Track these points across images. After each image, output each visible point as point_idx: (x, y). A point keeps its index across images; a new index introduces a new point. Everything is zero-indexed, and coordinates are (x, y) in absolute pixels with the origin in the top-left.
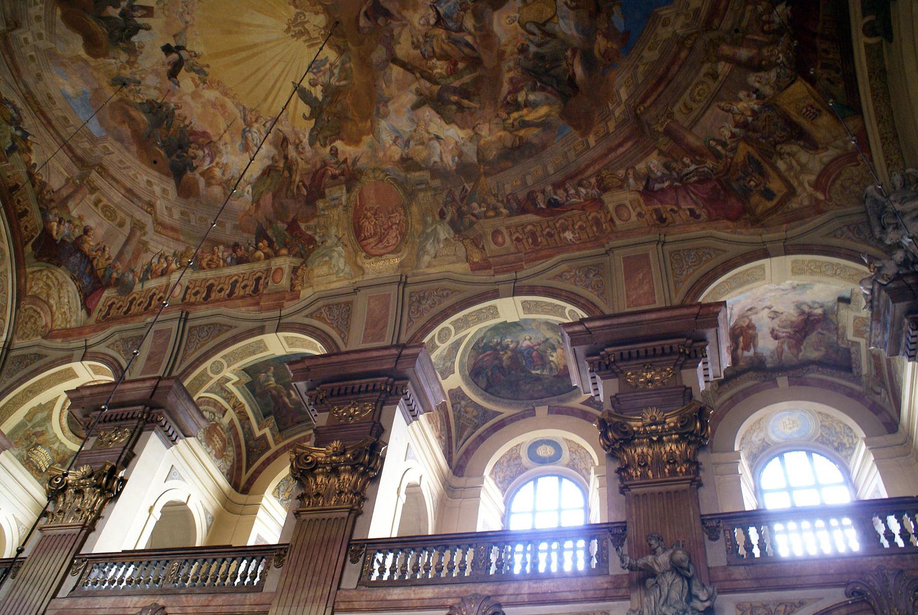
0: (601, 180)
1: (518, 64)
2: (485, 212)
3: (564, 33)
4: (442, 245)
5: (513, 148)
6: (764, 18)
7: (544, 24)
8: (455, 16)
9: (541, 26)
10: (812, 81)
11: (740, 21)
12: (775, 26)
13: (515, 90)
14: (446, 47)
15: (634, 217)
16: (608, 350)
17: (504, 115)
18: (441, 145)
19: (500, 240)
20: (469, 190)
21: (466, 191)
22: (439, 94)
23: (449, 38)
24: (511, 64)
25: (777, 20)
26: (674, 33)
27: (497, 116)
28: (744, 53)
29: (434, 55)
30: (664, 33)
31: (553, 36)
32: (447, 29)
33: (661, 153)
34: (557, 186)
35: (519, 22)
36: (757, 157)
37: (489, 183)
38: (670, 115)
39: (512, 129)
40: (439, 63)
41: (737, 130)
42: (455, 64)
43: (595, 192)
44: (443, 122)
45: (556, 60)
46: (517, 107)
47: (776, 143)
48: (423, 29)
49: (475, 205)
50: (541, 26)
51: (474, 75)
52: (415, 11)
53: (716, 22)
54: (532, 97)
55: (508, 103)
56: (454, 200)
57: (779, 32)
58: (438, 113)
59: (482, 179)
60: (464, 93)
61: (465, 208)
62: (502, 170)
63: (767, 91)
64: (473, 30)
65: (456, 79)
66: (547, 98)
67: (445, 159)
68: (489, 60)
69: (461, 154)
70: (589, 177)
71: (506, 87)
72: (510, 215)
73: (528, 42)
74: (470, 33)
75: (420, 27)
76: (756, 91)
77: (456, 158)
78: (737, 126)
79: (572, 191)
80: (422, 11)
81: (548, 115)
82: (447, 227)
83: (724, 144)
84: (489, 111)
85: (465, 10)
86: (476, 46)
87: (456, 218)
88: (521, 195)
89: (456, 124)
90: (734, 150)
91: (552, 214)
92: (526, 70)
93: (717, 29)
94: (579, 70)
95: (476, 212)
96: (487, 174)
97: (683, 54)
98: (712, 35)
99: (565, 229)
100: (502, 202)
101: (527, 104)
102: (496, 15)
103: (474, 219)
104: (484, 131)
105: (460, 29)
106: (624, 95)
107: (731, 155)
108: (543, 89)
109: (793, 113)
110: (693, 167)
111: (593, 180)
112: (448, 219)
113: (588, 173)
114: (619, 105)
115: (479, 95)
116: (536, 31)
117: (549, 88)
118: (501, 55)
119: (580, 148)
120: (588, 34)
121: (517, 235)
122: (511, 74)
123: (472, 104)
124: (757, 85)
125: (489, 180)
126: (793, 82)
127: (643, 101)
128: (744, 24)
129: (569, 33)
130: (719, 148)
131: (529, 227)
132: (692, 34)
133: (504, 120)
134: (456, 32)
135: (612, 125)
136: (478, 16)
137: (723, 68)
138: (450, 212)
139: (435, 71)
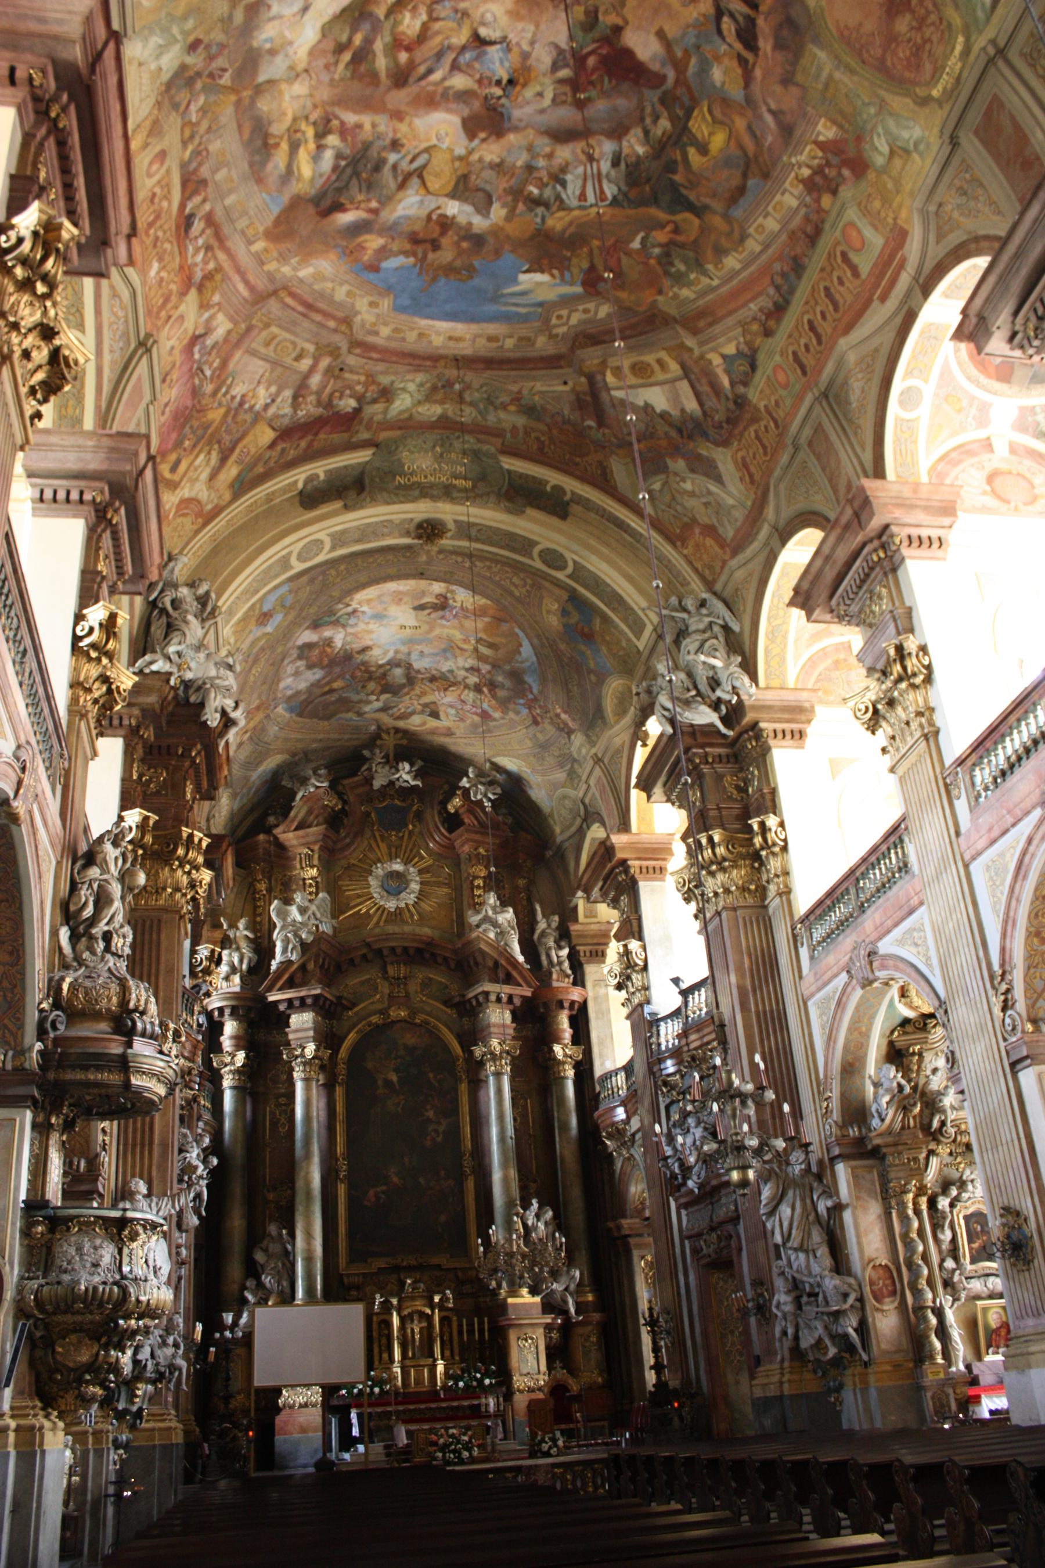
0: (208, 277)
1: (379, 137)
2: (190, 123)
3: (400, 201)
4: (153, 66)
5: (266, 136)
6: (348, 392)
7: (421, 177)
8: (477, 65)
9: (419, 173)
10: (272, 445)
11: (351, 372)
12: (335, 402)
13: (344, 131)
14: (438, 40)
15: (170, 344)
16: (123, 511)
17: (312, 118)
18: (294, 15)
19: (155, 167)
20: (222, 82)
21: (220, 77)
22: (371, 15)
23: (450, 47)
24: (382, 128)
25: (342, 403)
26: (357, 313)
27: (315, 106)
28: (315, 380)
29: (433, 18)
30: (362, 304)
31: (402, 186)
32: (463, 49)
33: (229, 332)
34: (210, 220)
35: (435, 146)
36: (210, 431)
37: (227, 113)
38: (267, 325)
39: (293, 130)
40: (417, 25)
41: (238, 399)
42: (408, 49)
43: (198, 275)
44: (326, 18)
45: (370, 186)
46: (320, 136)
47: (219, 442)
48: (476, 15)
49: (201, 100)
50: (419, 173)
51: (383, 75)
52: (510, 13)
53: (358, 351)
54: (328, 155)
55: (329, 121)
56: (211, 58)
57: (329, 405)
58: (344, 11)
59: (233, 98)
60: (362, 56)
61: (199, 85)
62: (240, 127)
63: (271, 411)
64: (447, 83)
65: (385, 46)
66: (321, 175)
67: (271, 24)
68: (398, 98)
69: (273, 52)
70: (216, 259)
71: (351, 118)
72: (183, 166)
73: (404, 151)
74: (444, 79)
75: (481, 10)
76: (273, 401)
77: (268, 46)
78: (243, 396)
79: (200, 241)
80: (504, 20)
81: (299, 179)
82: (176, 64)
83: (227, 392)
84: (325, 94)
85: (480, 82)
86: (423, 83)
87: (187, 75)
88: (205, 172)
89: (320, 42)
90: (220, 405)
91: (178, 227)
92: (367, 146)
93: (350, 352)
94: (346, 218)
95: (193, 108)
96: (238, 103)
97: (332, 324)
98: (344, 346)
99: (160, 259)
100: (200, 144)
101: (320, 148)
102: (456, 120)
103: (182, 108)
104: (300, 88)
105: (455, 67)
106: (305, 273)
107: (216, 404)
108: (335, 168)
109: (244, 442)
110: (208, 373)
111: (211, 266)
112: (189, 60)
113: (221, 256)
114: (295, 269)
115: (352, 78)
116: (415, 165)
117: (334, 178)
118: (398, 116)
119: (250, 232)
120: (390, 230)
121: (157, 190)
122: (368, 127)
123: (341, 66)
124: (279, 400)
125: (230, 110)
126: (274, 429)
127: (292, 295)
128: (347, 375)
129: (400, 206)
130: (224, 390)
131: (165, 204)
132: (351, 329)
133: (307, 118)
134: (455, 60)
135: (271, 267)
136: (464, 96)
137: (305, 364)
138: (195, 61)
139: (408, 15)
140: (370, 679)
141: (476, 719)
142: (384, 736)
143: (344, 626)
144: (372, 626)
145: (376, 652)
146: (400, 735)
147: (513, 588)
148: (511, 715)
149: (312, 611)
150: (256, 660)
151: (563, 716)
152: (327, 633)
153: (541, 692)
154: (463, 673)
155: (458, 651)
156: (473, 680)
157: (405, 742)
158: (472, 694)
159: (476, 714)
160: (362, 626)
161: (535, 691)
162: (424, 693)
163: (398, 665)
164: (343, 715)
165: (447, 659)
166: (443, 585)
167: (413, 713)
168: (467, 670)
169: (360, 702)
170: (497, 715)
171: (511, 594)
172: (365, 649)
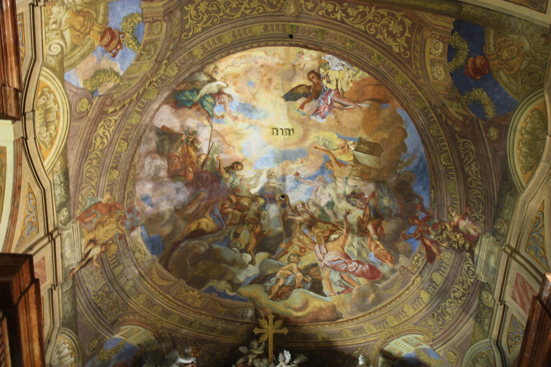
140: (243, 221)
141: (363, 281)
142: (263, 322)
143: (210, 116)
144: (241, 125)
145: (246, 173)
146: (279, 323)
147: (391, 42)
148: (403, 260)
149: (173, 72)
150: (102, 113)
151: (463, 224)
152: (192, 123)
153: (434, 201)
154: (343, 205)
155: (336, 168)
156: (357, 214)
157: (285, 331)
158: (356, 239)
159: (362, 275)
160: (227, 124)
161: (426, 204)
162: (303, 250)
163: (272, 199)
164: (213, 283)
165: (325, 184)
166: (314, 53)
167: (292, 287)
168: (348, 198)
169: (233, 263)
170: (385, 269)
171: (387, 50)
172: (235, 166)
